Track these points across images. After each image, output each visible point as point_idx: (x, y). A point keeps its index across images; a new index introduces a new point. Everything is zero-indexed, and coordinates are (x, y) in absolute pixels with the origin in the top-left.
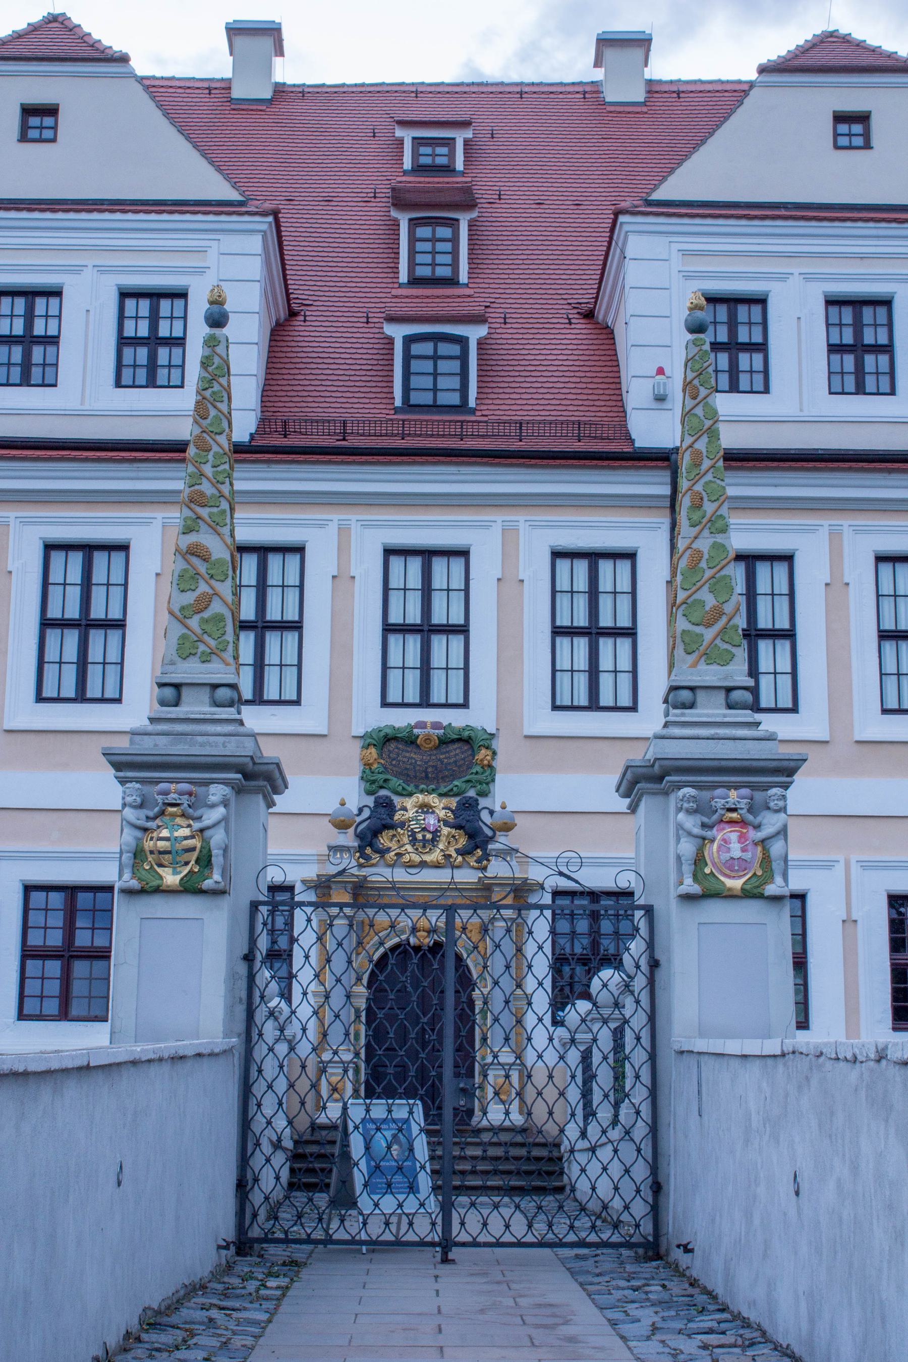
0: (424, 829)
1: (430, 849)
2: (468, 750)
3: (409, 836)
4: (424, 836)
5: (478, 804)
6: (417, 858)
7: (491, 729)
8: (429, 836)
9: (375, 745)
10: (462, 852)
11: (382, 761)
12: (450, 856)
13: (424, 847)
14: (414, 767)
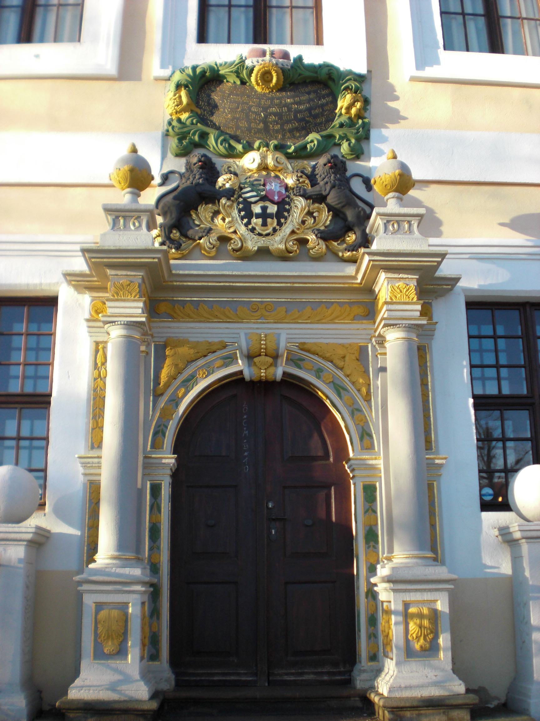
0: (264, 198)
1: (275, 230)
2: (328, 95)
3: (240, 211)
4: (264, 209)
5: (345, 170)
6: (253, 244)
7: (361, 69)
8: (273, 209)
9: (186, 86)
10: (326, 236)
11: (199, 111)
12: (307, 241)
13: (264, 224)
14: (247, 116)
